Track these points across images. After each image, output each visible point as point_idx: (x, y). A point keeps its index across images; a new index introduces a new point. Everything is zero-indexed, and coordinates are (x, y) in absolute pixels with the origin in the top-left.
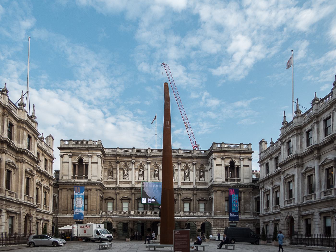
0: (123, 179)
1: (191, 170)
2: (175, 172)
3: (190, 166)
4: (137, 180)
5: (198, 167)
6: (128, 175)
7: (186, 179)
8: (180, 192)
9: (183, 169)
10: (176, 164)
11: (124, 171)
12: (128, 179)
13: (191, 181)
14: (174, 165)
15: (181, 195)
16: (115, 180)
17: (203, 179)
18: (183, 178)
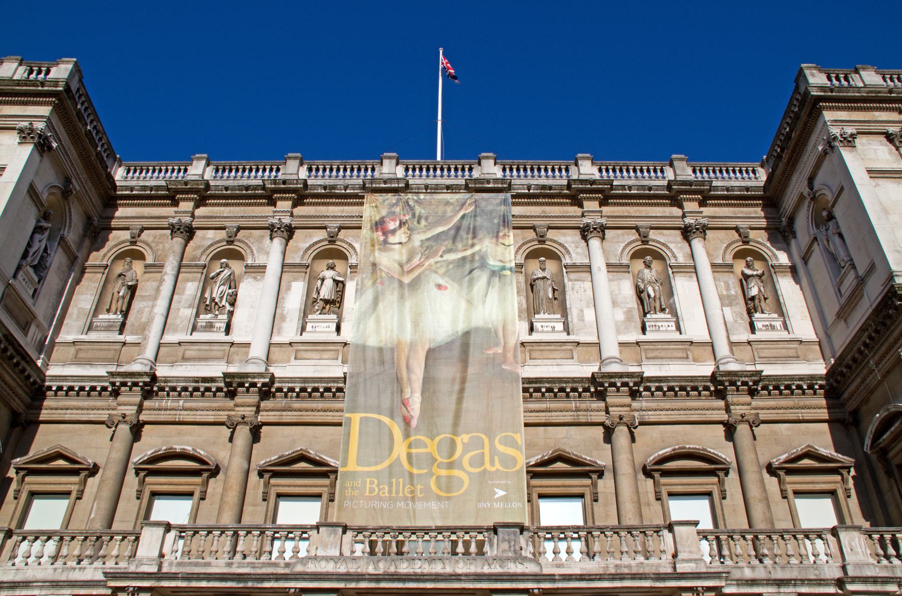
0: (194, 329)
1: (680, 269)
2: (568, 284)
3: (669, 248)
4: (289, 332)
5: (725, 253)
6: (228, 307)
7: (657, 320)
8: (618, 400)
9: (621, 266)
10: (569, 239)
11: (208, 281)
12: (228, 330)
13: (695, 330)
14: (560, 244)
15: (631, 428)
16: (130, 338)
17: (774, 319)
18: (629, 318)
